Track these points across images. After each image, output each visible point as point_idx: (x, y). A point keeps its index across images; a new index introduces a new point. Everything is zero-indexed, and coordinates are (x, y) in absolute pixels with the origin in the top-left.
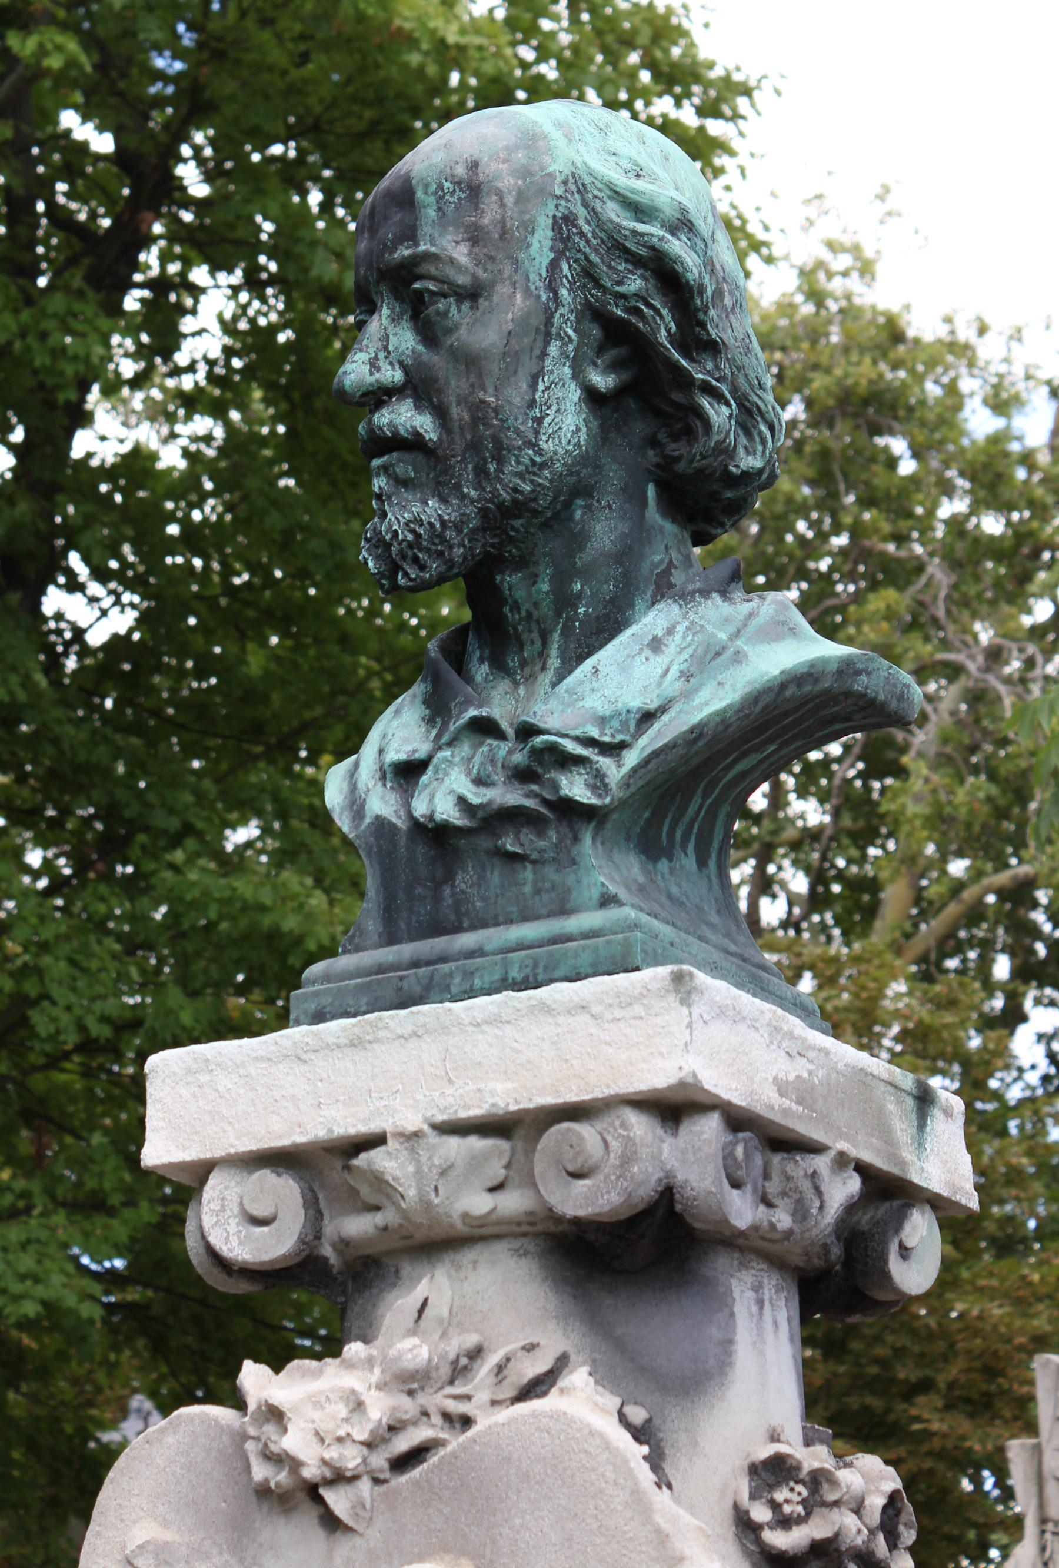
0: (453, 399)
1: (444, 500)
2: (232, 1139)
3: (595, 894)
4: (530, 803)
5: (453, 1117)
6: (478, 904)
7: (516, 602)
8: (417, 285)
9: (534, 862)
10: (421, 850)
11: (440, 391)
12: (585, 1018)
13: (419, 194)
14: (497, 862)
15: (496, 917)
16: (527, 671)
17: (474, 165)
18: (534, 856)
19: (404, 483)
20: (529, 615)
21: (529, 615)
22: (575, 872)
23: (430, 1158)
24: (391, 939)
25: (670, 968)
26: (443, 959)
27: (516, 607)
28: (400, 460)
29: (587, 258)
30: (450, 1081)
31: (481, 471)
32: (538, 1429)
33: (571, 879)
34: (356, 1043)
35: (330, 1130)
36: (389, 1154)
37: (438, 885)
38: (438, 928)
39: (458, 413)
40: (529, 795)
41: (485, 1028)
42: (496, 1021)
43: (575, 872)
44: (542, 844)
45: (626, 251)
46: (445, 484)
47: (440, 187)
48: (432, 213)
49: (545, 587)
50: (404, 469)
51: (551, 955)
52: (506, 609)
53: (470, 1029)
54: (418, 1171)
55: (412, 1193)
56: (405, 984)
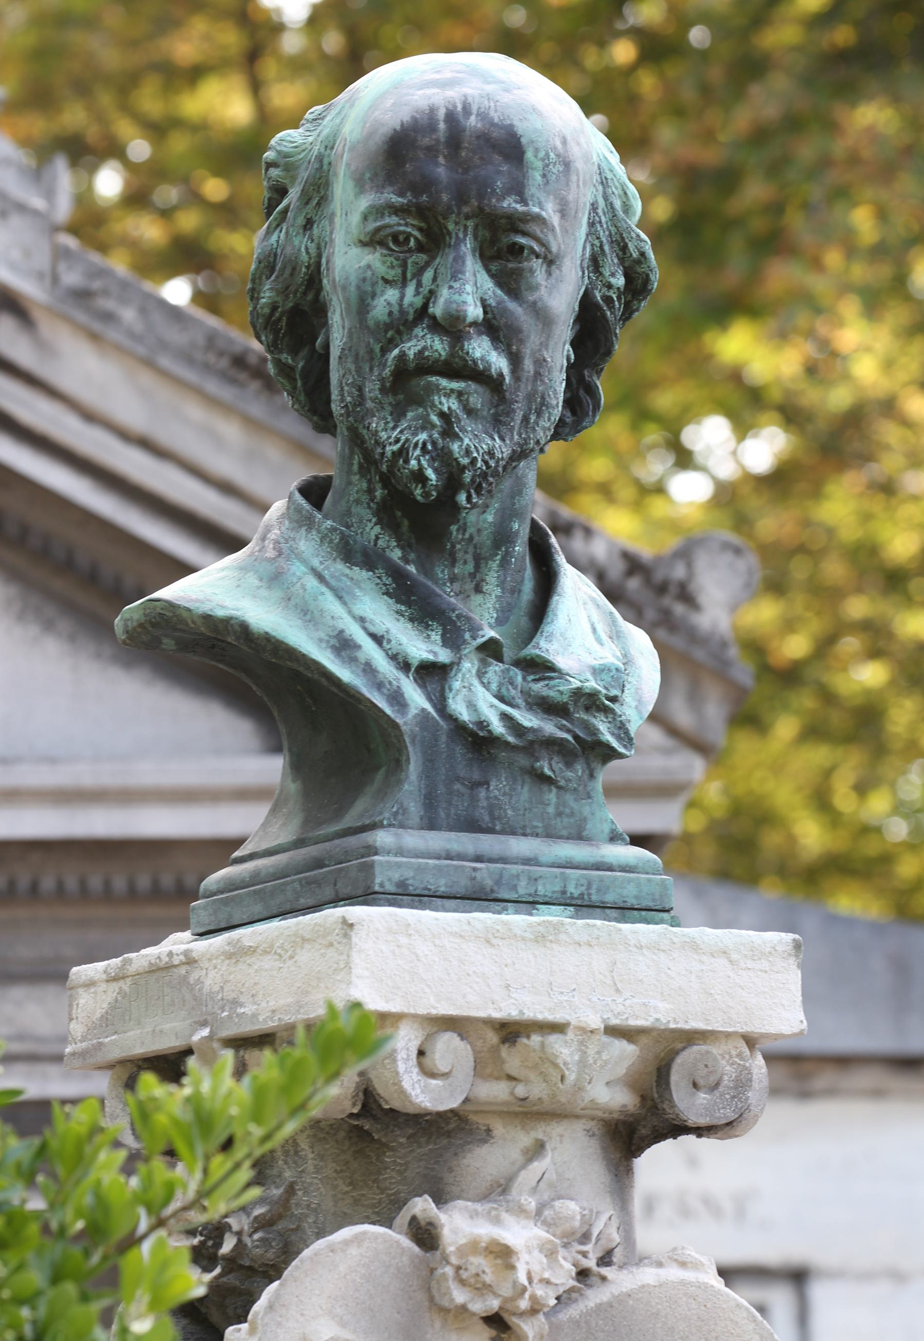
0: (528, 351)
1: (502, 439)
2: (432, 1000)
3: (606, 828)
4: (570, 738)
5: (624, 1023)
6: (510, 812)
7: (465, 524)
8: (522, 240)
9: (560, 788)
10: (459, 750)
11: (521, 342)
12: (722, 962)
13: (529, 155)
14: (527, 778)
15: (524, 827)
16: (457, 587)
17: (564, 142)
18: (562, 783)
19: (470, 412)
20: (471, 538)
21: (471, 538)
22: (590, 804)
23: (598, 1053)
24: (431, 824)
25: (790, 936)
26: (503, 860)
27: (463, 529)
28: (476, 392)
29: (601, 247)
30: (618, 991)
31: (526, 419)
32: (685, 1294)
33: (586, 811)
34: (540, 939)
35: (521, 1012)
36: (566, 1042)
37: (475, 785)
38: (472, 826)
39: (528, 365)
40: (561, 728)
41: (645, 951)
42: (655, 948)
43: (590, 804)
44: (569, 774)
45: (624, 248)
46: (505, 424)
47: (547, 155)
48: (538, 176)
49: (490, 518)
50: (478, 397)
51: (601, 880)
52: (454, 528)
53: (634, 949)
54: (583, 1063)
55: (571, 1077)
56: (478, 875)
